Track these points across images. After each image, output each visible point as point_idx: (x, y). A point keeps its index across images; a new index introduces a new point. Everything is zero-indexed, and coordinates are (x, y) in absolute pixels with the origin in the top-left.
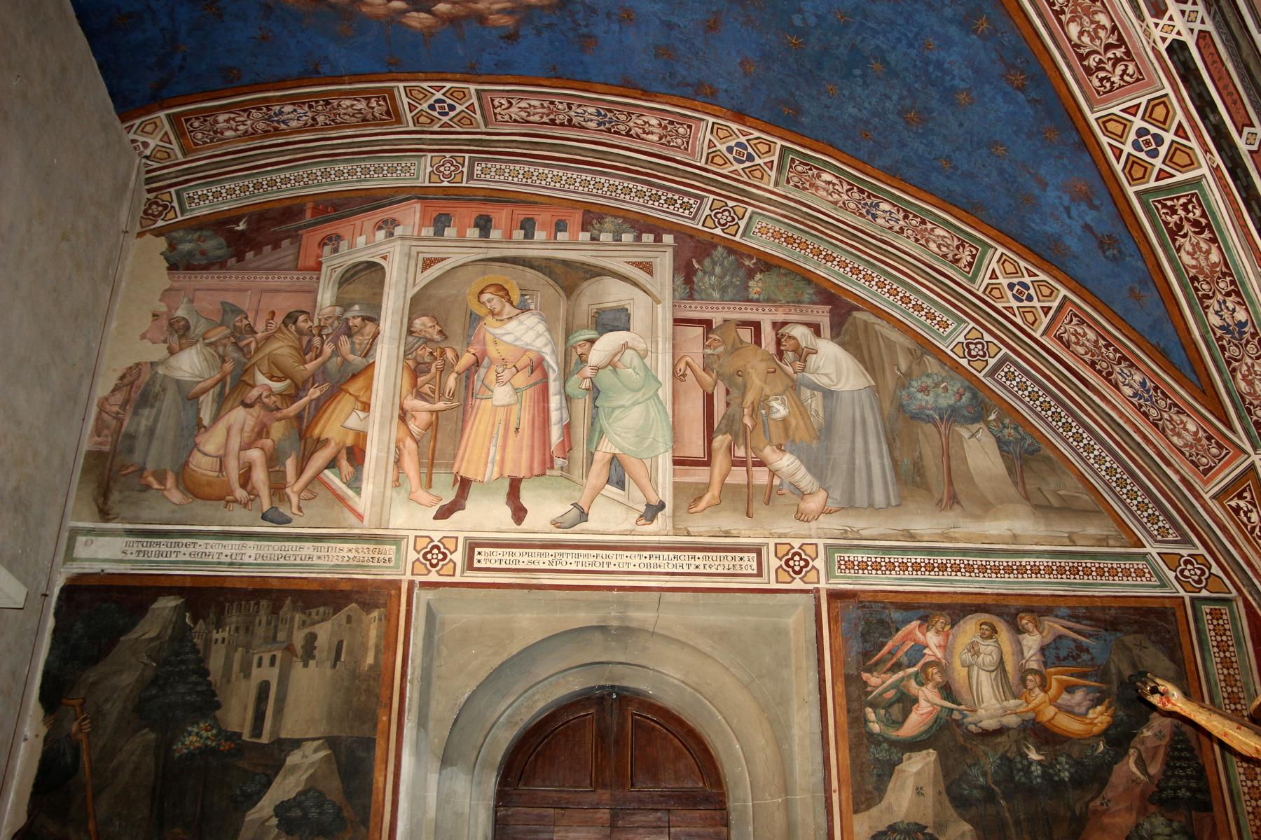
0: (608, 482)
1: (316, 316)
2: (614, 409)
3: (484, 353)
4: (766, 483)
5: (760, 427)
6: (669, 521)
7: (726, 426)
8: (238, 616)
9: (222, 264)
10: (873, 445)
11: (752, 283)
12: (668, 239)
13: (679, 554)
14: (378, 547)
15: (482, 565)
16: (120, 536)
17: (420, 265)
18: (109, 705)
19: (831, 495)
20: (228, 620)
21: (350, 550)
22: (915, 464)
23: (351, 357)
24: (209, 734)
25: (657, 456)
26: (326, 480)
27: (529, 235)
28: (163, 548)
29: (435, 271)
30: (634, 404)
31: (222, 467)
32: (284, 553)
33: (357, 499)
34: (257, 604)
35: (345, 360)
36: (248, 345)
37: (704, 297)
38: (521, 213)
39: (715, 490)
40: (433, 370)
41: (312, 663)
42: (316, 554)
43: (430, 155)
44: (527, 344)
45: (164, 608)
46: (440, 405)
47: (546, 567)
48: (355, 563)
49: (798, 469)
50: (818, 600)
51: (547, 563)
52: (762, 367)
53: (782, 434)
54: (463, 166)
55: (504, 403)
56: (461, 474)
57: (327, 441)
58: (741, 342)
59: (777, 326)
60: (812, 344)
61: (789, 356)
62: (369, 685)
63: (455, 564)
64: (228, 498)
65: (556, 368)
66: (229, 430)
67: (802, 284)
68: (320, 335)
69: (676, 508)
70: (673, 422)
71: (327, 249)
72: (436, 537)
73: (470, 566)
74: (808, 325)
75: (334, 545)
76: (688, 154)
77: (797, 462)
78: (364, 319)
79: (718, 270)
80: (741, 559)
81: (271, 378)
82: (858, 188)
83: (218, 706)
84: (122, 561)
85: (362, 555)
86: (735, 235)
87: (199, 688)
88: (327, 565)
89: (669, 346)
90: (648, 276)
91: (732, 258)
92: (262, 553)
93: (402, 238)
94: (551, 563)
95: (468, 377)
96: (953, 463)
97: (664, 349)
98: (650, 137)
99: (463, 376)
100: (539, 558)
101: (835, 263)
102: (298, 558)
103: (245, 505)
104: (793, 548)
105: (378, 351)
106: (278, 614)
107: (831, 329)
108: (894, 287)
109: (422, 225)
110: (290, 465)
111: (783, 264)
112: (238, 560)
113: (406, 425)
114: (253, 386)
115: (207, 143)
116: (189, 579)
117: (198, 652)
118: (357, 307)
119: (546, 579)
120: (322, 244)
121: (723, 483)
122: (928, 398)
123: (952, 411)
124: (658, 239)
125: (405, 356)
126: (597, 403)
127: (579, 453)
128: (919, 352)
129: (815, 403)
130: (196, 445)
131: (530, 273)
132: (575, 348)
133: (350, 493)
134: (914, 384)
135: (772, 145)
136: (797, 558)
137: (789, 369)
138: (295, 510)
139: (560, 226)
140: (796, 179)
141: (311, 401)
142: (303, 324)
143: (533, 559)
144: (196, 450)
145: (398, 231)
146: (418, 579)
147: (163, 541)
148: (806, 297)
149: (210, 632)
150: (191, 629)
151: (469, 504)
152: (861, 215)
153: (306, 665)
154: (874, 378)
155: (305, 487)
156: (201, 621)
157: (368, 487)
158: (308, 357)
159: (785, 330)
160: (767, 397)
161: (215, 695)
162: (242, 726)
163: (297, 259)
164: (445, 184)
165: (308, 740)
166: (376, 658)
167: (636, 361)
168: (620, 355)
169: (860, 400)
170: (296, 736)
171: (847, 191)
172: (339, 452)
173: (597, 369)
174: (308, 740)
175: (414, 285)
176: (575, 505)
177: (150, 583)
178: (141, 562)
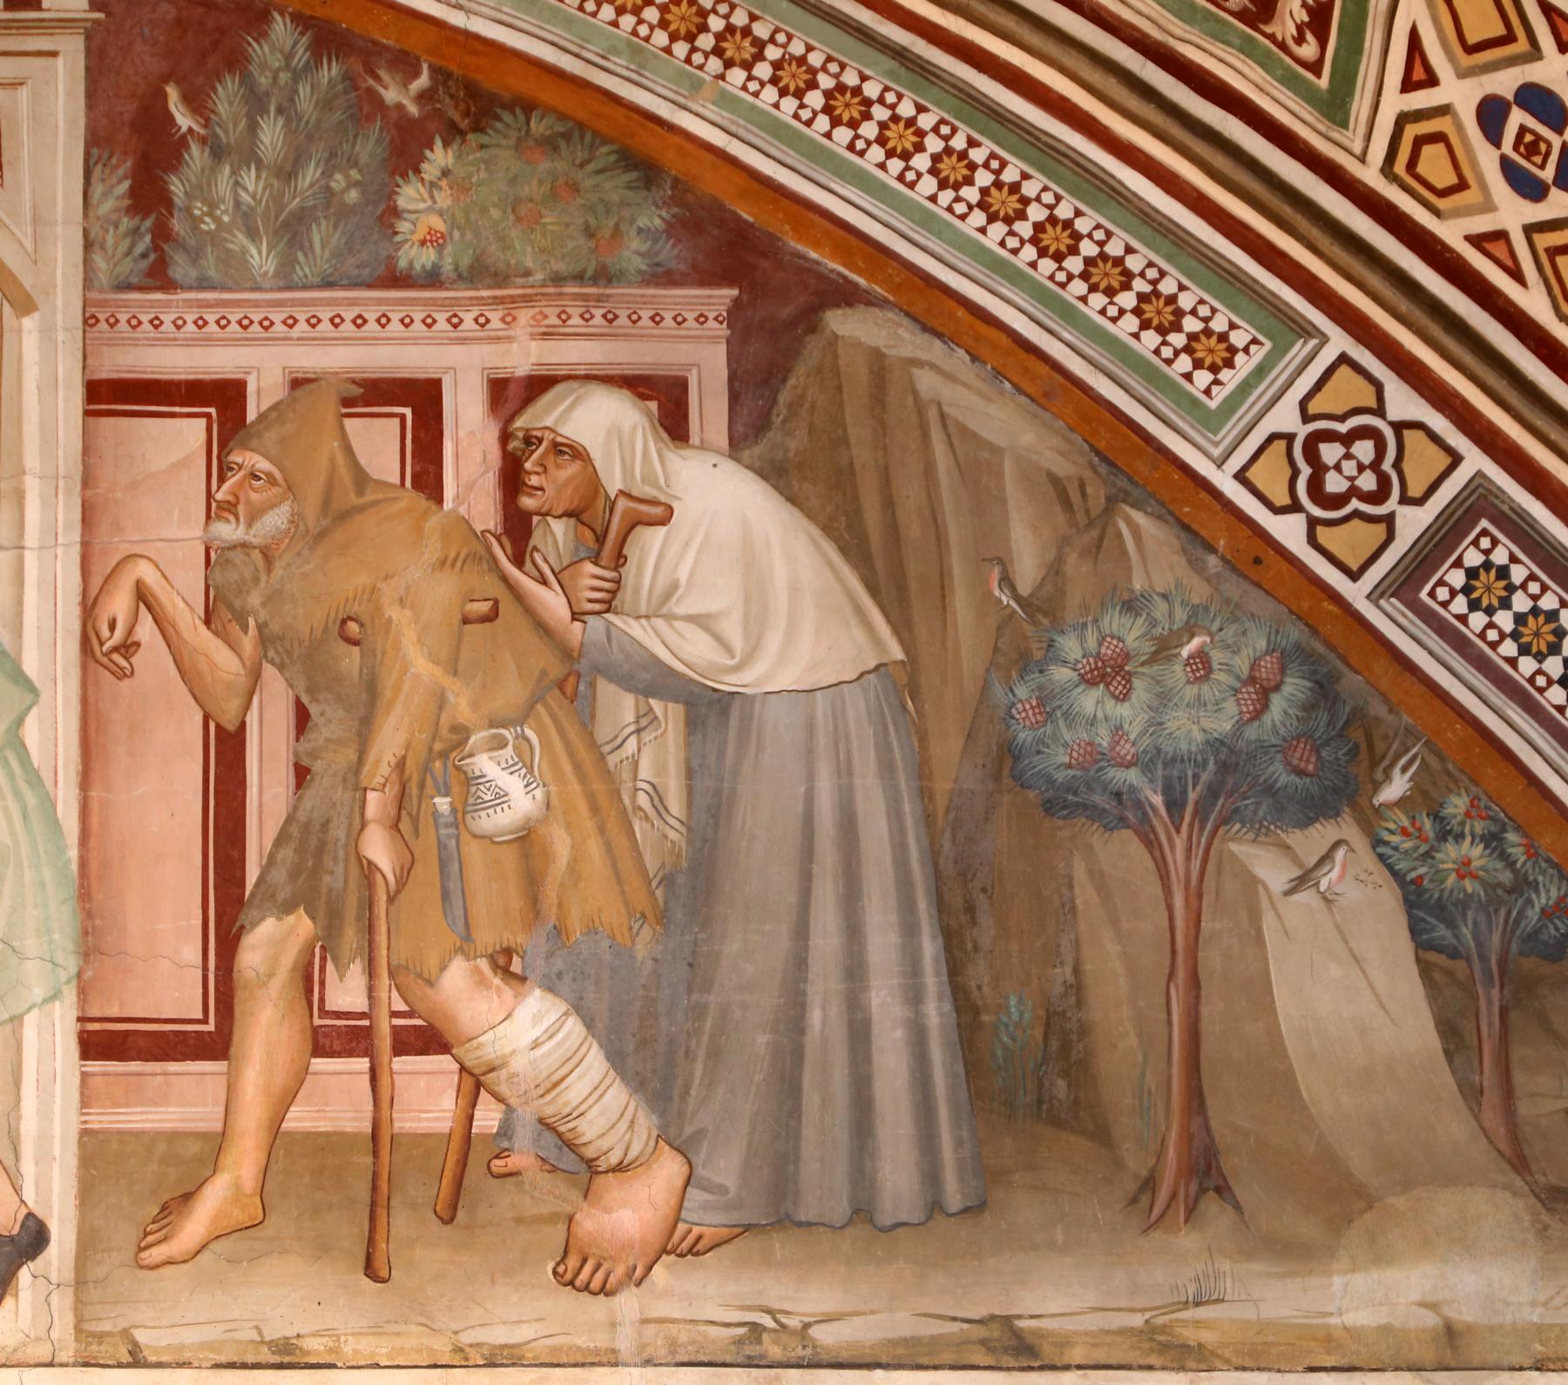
4: (444, 1126)
5: (427, 872)
7: (294, 874)
10: (882, 944)
11: (409, 195)
19: (700, 1171)
22: (1052, 1019)
37: (211, 268)
49: (573, 1061)
53: (517, 903)
58: (361, 479)
60: (649, 479)
61: (556, 535)
67: (615, 187)
70: (83, 863)
74: (637, 385)
77: (574, 1026)
79: (271, 135)
89: (68, 512)
91: (330, 72)
96: (1211, 1011)
97: (50, 529)
101: (763, 70)
107: (734, 398)
108: (1010, 175)
111: (547, 94)
122: (1123, 711)
123: (1224, 768)
128: (1097, 494)
134: (1070, 646)
137: (553, 603)
148: (633, 254)
154: (902, 627)
159: (543, 416)
160: (461, 733)
169: (839, 735)
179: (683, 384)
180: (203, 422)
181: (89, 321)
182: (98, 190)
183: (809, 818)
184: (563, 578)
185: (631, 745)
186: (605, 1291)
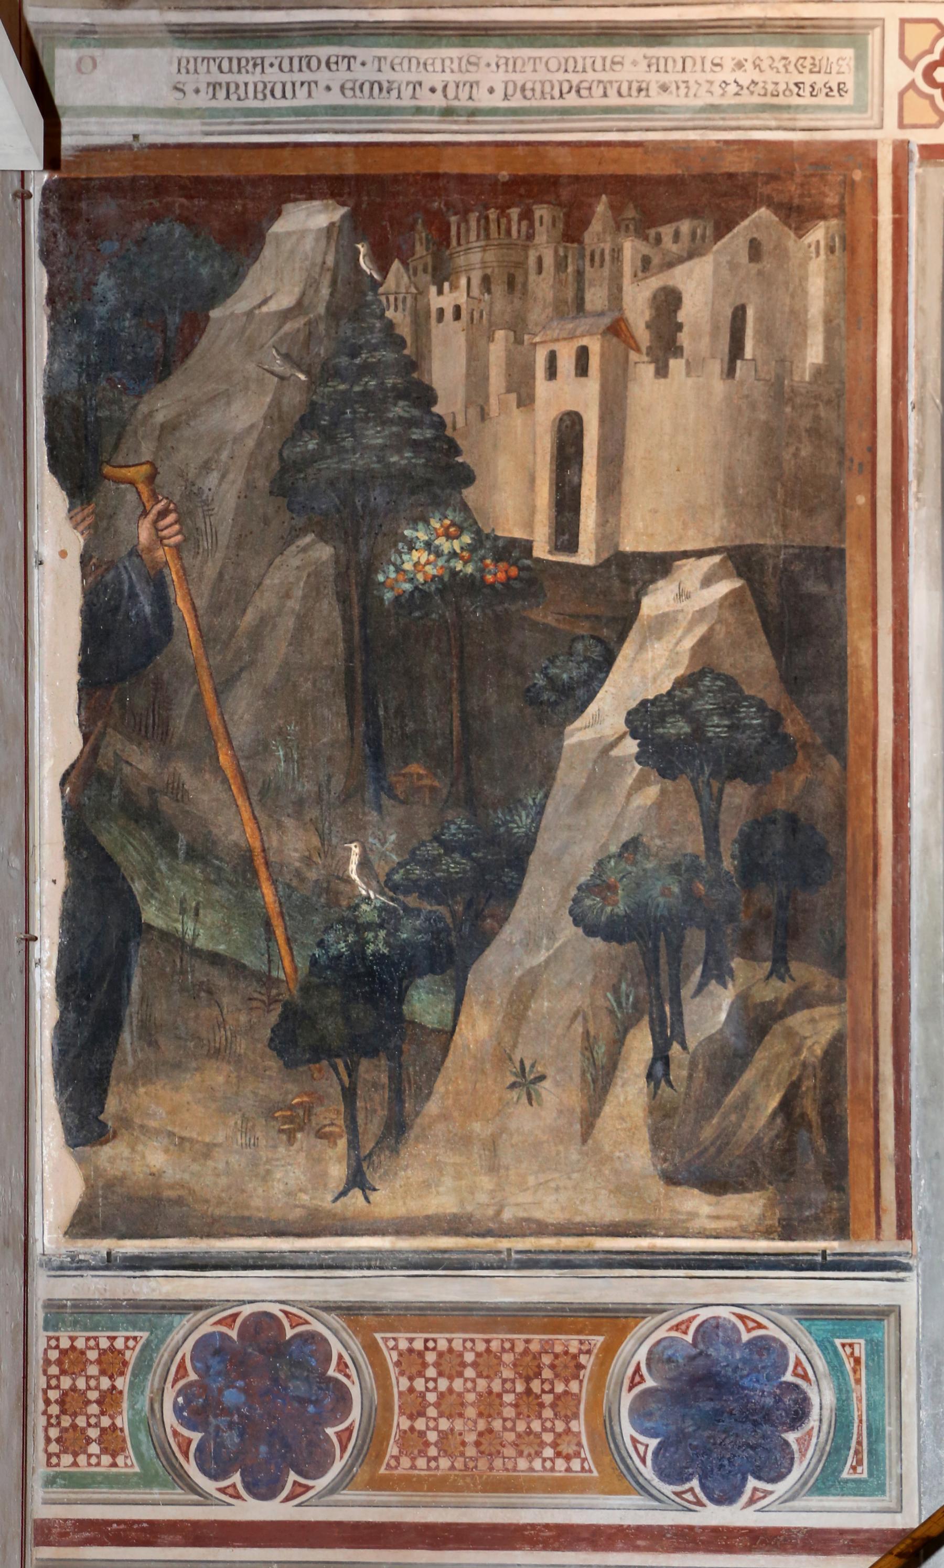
8: (484, 249)
14: (808, 52)
16: (159, 43)
18: (212, 479)
20: (461, 261)
21: (740, 65)
24: (456, 545)
28: (272, 75)
32: (575, 79)
34: (527, 215)
41: (676, 365)
42: (654, 79)
45: (303, 234)
48: (756, 100)
62: (817, 418)
75: (696, 52)
83: (466, 477)
84: (176, 113)
85: (770, 76)
87: (416, 434)
88: (687, 109)
92: (519, 78)
102: (612, 92)
106: (580, 242)
112: (464, 102)
116: (350, 154)
117: (402, 343)
147: (270, 54)
149: (421, 293)
150: (375, 285)
153: (662, 371)
156: (396, 265)
161: (457, 451)
162: (530, 525)
165: (686, 555)
166: (828, 349)
170: (658, 547)
174: (686, 555)
177: (257, 167)
178: (224, 112)
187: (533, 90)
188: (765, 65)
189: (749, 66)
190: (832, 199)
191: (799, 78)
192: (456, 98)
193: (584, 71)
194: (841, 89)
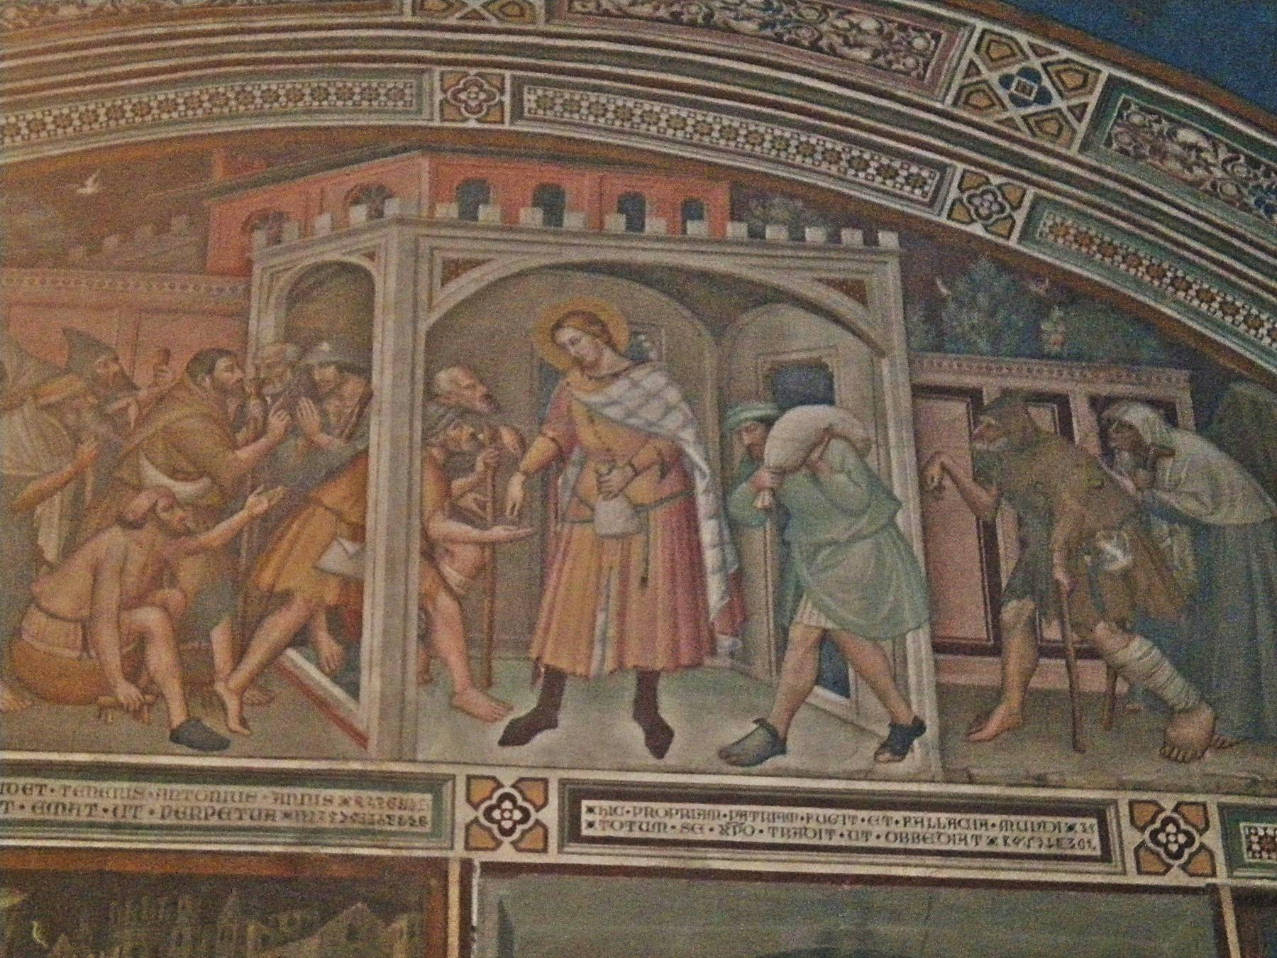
0: (818, 681)
1: (249, 361)
2: (819, 547)
3: (573, 439)
4: (1103, 689)
6: (934, 756)
9: (59, 260)
12: (888, 239)
13: (958, 816)
14: (397, 795)
15: (597, 832)
17: (438, 271)
23: (323, 438)
25: (903, 636)
26: (288, 664)
27: (635, 224)
29: (467, 284)
30: (855, 538)
31: (87, 642)
32: (218, 807)
33: (351, 704)
35: (313, 448)
36: (125, 409)
38: (619, 184)
39: (1013, 698)
40: (480, 466)
43: (438, 70)
44: (651, 424)
46: (499, 532)
47: (715, 836)
48: (356, 826)
50: (1218, 905)
51: (717, 829)
52: (1080, 477)
54: (502, 91)
55: (615, 530)
56: (547, 659)
57: (286, 597)
58: (1037, 430)
59: (1098, 404)
63: (546, 830)
64: (103, 700)
65: (708, 471)
66: (96, 571)
68: (259, 395)
69: (944, 732)
71: (260, 237)
72: (508, 778)
73: (572, 832)
74: (1152, 403)
75: (313, 791)
76: (922, 87)
77: (1156, 652)
78: (341, 368)
80: (1071, 828)
81: (173, 473)
82: (1247, 156)
85: (367, 810)
86: (1008, 237)
89: (907, 435)
90: (860, 309)
91: (1005, 279)
92: (174, 805)
93: (401, 221)
94: (724, 831)
95: (545, 484)
98: (856, 53)
99: (537, 478)
100: (701, 821)
102: (247, 817)
103: (137, 714)
104: (1162, 810)
105: (374, 429)
109: (435, 198)
110: (220, 639)
112: (130, 819)
113: (437, 568)
114: (139, 489)
115: (22, 27)
118: (325, 346)
119: (718, 862)
120: (249, 227)
121: (1025, 685)
124: (871, 240)
125: (423, 439)
126: (789, 535)
127: (762, 627)
129: (1178, 546)
130: (33, 600)
131: (647, 296)
132: (739, 432)
133: (338, 692)
135: (1092, 74)
136: (1171, 828)
137: (1128, 484)
138: (234, 724)
139: (691, 210)
140: (1126, 139)
141: (253, 518)
142: (227, 375)
143: (690, 822)
144: (33, 609)
145: (392, 208)
146: (479, 858)
151: (565, 718)
152: (1245, 207)
155: (252, 681)
156: (62, 938)
157: (371, 683)
158: (240, 437)
159: (1114, 412)
160: (1092, 535)
163: (203, 255)
164: (472, 124)
167: (851, 460)
168: (821, 448)
171: (1225, 162)
172: (312, 616)
173: (782, 472)
175: (431, 308)
176: (761, 722)
179: (1174, 404)
180: (964, 405)
181: (911, 362)
182: (910, 313)
183: (1250, 576)
184: (1132, 475)
185: (1169, 541)
186: (1183, 761)
187: (184, 813)
188: (365, 803)
189: (352, 803)
190: (413, 898)
191: (391, 813)
192: (124, 816)
193: (225, 801)
194: (422, 821)
